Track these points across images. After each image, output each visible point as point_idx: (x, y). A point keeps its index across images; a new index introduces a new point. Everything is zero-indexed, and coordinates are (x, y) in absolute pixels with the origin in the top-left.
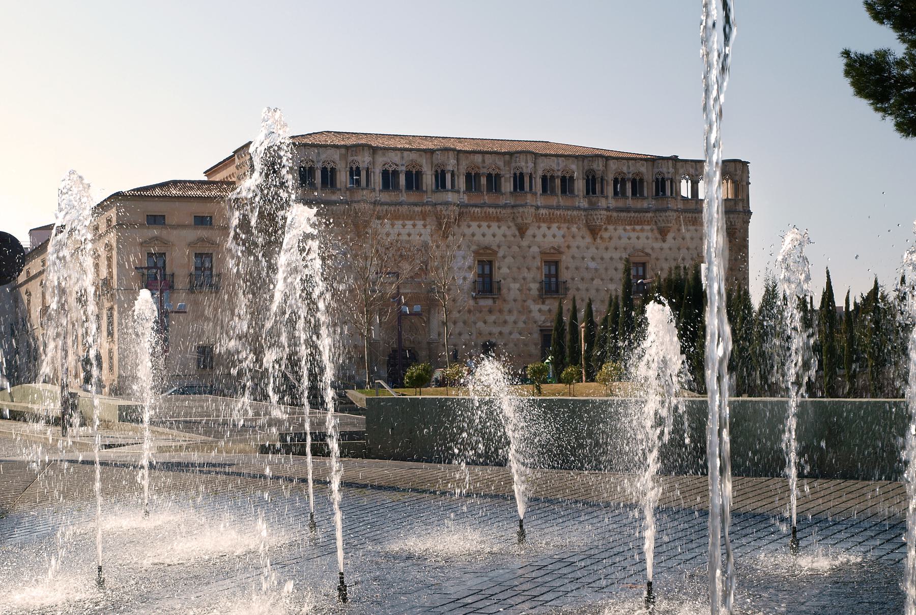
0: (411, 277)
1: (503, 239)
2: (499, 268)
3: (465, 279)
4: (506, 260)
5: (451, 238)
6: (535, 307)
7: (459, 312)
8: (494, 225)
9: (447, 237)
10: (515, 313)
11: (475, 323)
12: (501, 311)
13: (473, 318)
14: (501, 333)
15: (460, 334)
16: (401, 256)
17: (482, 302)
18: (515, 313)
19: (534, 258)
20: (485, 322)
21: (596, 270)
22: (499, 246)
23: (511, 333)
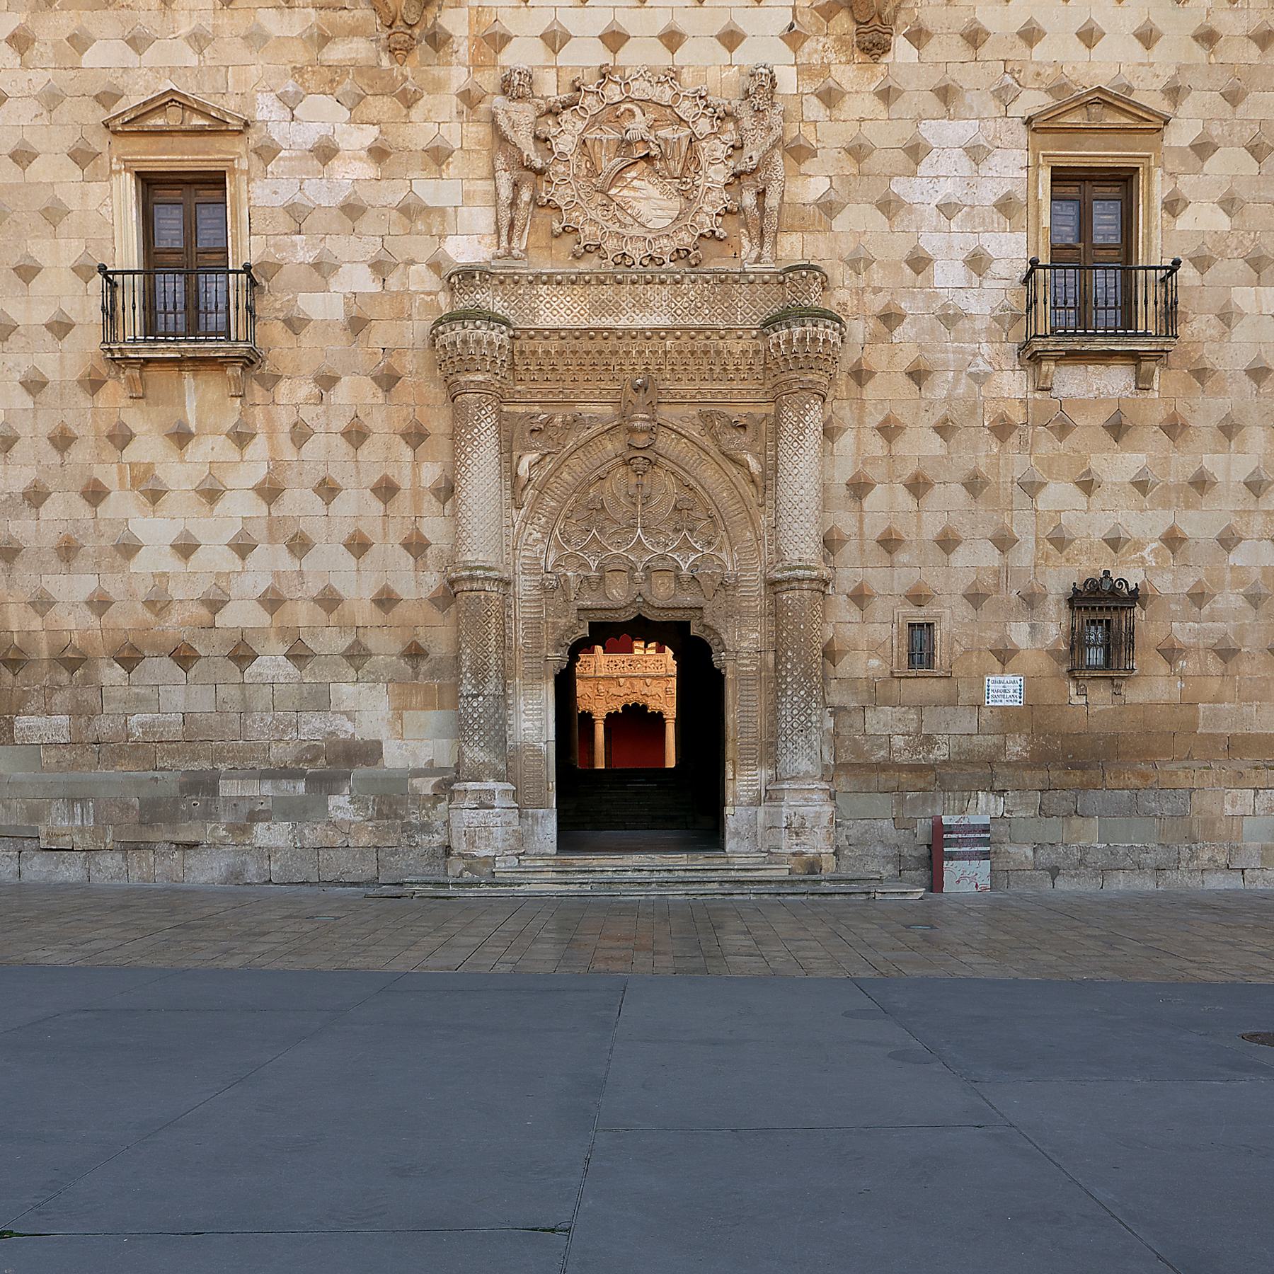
0: (680, 255)
1: (1199, 53)
2: (1173, 206)
3: (977, 262)
4: (1213, 164)
5: (902, 50)
7: (943, 429)
9: (885, 48)
11: (1032, 488)
12: (1174, 429)
13: (1017, 463)
14: (1173, 540)
15: (947, 543)
16: (625, 145)
17: (1073, 382)
20: (1087, 485)
22: (1174, 93)
23: (1228, 541)
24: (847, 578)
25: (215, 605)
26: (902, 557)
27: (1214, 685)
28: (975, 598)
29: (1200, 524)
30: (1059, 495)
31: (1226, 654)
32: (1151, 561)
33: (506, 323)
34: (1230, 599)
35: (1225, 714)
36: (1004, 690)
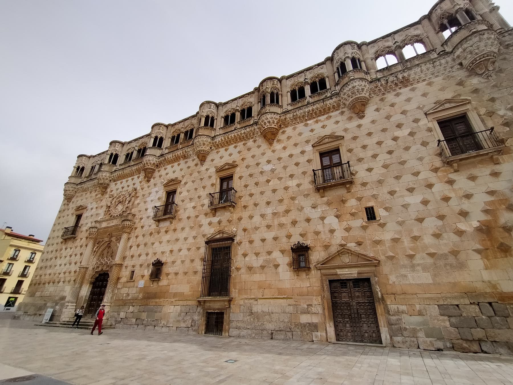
6: (204, 221)
8: (182, 162)
10: (187, 229)
11: (153, 244)
13: (151, 239)
18: (187, 229)
19: (210, 177)
20: (160, 243)
21: (273, 171)
24: (125, 264)
25: (60, 274)
26: (134, 259)
27: (173, 281)
28: (141, 266)
29: (176, 248)
30: (157, 244)
31: (176, 274)
32: (168, 255)
33: (96, 228)
34: (179, 262)
35: (175, 288)
36: (141, 284)
